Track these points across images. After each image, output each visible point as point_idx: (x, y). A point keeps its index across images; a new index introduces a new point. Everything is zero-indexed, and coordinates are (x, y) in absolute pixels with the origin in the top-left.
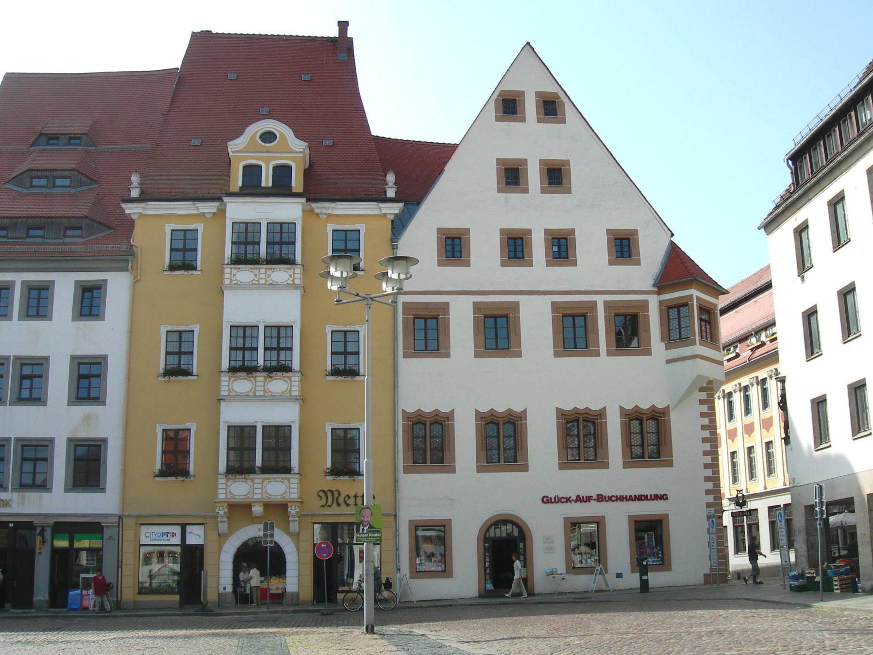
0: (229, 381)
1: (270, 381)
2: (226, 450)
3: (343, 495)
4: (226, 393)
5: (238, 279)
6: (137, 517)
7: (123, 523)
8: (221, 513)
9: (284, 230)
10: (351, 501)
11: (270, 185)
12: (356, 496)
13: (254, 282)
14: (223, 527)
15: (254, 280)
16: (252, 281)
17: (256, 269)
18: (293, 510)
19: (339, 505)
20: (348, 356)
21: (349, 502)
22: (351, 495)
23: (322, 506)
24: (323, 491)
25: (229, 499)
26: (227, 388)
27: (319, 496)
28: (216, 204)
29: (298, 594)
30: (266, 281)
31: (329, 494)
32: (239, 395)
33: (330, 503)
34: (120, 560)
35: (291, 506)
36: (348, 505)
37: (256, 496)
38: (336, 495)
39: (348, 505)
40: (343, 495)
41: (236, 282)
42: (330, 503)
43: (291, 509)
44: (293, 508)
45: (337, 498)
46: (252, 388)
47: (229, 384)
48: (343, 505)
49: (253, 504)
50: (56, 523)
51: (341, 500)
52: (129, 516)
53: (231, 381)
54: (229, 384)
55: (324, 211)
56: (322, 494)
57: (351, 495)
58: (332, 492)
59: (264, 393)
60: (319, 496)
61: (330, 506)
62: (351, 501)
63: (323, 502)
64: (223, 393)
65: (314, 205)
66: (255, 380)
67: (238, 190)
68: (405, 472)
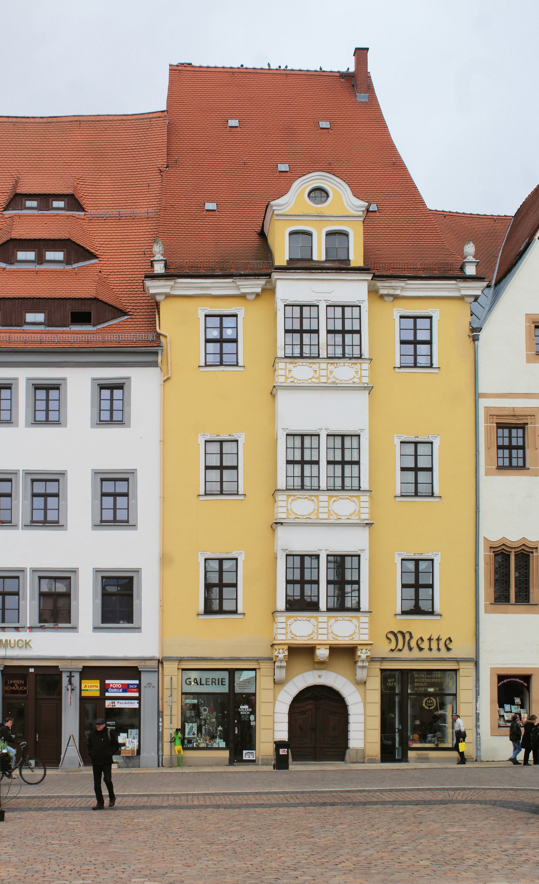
0: (287, 501)
1: (334, 501)
2: (285, 583)
3: (416, 637)
4: (284, 516)
5: (295, 376)
6: (180, 660)
7: (163, 667)
8: (281, 656)
9: (346, 316)
10: (425, 645)
11: (323, 258)
12: (430, 639)
13: (314, 380)
14: (280, 674)
15: (313, 377)
16: (310, 379)
17: (315, 363)
18: (362, 654)
19: (410, 649)
20: (419, 472)
21: (422, 646)
22: (426, 638)
23: (392, 650)
24: (392, 632)
25: (290, 640)
26: (284, 510)
27: (388, 638)
28: (262, 282)
29: (363, 751)
30: (328, 378)
31: (400, 637)
32: (299, 518)
33: (400, 646)
34: (161, 710)
35: (361, 649)
36: (421, 649)
37: (321, 637)
38: (407, 637)
39: (421, 649)
40: (416, 637)
41: (292, 380)
42: (400, 646)
43: (361, 653)
44: (364, 651)
45: (409, 640)
46: (315, 509)
47: (287, 504)
48: (416, 650)
49: (317, 647)
50: (84, 667)
51: (413, 644)
52: (170, 659)
53: (289, 502)
54: (287, 504)
55: (391, 292)
56: (391, 636)
57: (426, 638)
58: (403, 634)
59: (329, 516)
60: (388, 638)
61: (400, 650)
62: (425, 645)
63: (393, 646)
64: (281, 516)
65: (379, 284)
66: (318, 499)
67: (285, 264)
68: (486, 612)
